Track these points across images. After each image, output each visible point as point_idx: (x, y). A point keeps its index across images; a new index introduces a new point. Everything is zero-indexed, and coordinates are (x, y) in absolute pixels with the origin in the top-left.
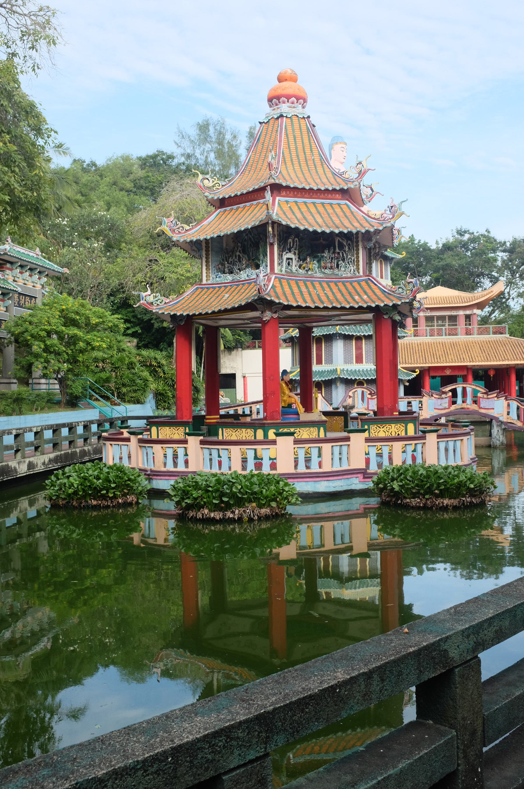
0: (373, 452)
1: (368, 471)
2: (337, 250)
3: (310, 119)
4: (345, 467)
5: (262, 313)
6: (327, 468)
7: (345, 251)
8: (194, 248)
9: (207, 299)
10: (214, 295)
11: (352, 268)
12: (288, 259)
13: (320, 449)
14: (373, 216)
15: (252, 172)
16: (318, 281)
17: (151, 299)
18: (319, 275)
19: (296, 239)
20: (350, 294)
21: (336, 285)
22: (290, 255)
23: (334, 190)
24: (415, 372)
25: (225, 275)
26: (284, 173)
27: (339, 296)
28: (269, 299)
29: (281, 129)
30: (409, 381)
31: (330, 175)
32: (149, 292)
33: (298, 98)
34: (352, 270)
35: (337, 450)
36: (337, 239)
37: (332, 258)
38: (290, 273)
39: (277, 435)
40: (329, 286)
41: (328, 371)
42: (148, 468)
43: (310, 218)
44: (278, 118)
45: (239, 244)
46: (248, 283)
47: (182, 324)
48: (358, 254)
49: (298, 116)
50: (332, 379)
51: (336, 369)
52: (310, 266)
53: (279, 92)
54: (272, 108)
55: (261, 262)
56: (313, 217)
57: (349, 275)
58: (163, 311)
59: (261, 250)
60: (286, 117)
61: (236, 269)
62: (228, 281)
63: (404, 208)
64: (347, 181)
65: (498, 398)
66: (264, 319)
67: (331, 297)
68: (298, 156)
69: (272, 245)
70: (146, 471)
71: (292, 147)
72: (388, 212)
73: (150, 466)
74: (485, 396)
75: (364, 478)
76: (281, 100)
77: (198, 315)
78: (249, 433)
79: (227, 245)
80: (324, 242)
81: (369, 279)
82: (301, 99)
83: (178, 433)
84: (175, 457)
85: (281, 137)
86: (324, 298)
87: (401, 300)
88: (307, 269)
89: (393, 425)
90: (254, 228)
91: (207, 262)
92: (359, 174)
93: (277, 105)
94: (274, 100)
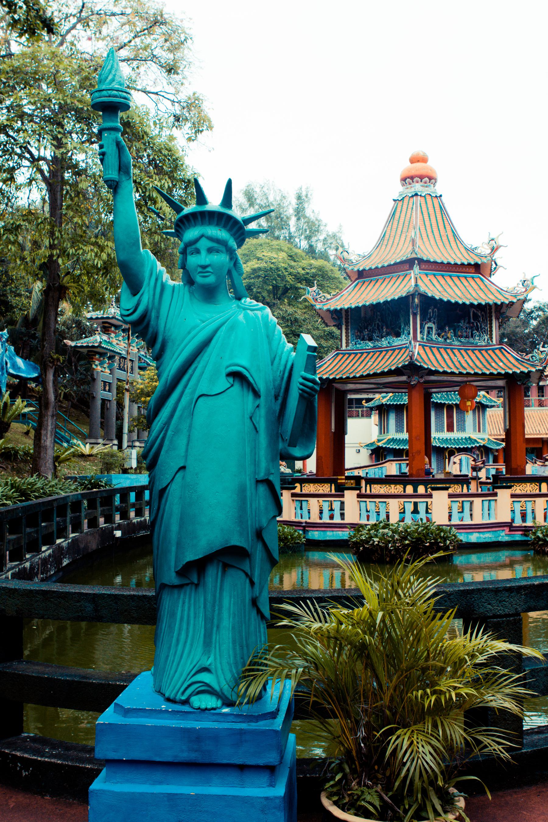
0: (518, 508)
1: (514, 525)
2: (472, 321)
3: (442, 198)
5: (409, 377)
7: (479, 321)
8: (334, 316)
9: (351, 365)
10: (357, 361)
11: (486, 337)
12: (428, 328)
13: (472, 503)
14: (505, 289)
15: (389, 247)
18: (456, 343)
20: (487, 360)
21: (474, 353)
23: (469, 264)
26: (422, 248)
27: (478, 363)
28: (419, 364)
29: (416, 207)
31: (463, 250)
33: (430, 178)
35: (486, 504)
36: (472, 310)
37: (467, 328)
38: (430, 340)
39: (433, 489)
42: (303, 520)
43: (449, 290)
44: (412, 196)
45: (379, 313)
46: (391, 350)
48: (491, 324)
49: (430, 195)
52: (449, 335)
53: (413, 173)
56: (451, 288)
57: (484, 344)
59: (402, 319)
60: (421, 196)
63: (536, 282)
64: (480, 256)
67: (471, 364)
68: (432, 232)
69: (415, 315)
70: (302, 523)
71: (427, 223)
72: (521, 286)
73: (305, 519)
75: (510, 531)
76: (415, 180)
79: (365, 314)
80: (460, 313)
82: (431, 178)
83: (325, 489)
85: (416, 214)
86: (465, 365)
89: (528, 484)
90: (400, 299)
91: (347, 329)
92: (492, 250)
93: (410, 184)
94: (408, 180)
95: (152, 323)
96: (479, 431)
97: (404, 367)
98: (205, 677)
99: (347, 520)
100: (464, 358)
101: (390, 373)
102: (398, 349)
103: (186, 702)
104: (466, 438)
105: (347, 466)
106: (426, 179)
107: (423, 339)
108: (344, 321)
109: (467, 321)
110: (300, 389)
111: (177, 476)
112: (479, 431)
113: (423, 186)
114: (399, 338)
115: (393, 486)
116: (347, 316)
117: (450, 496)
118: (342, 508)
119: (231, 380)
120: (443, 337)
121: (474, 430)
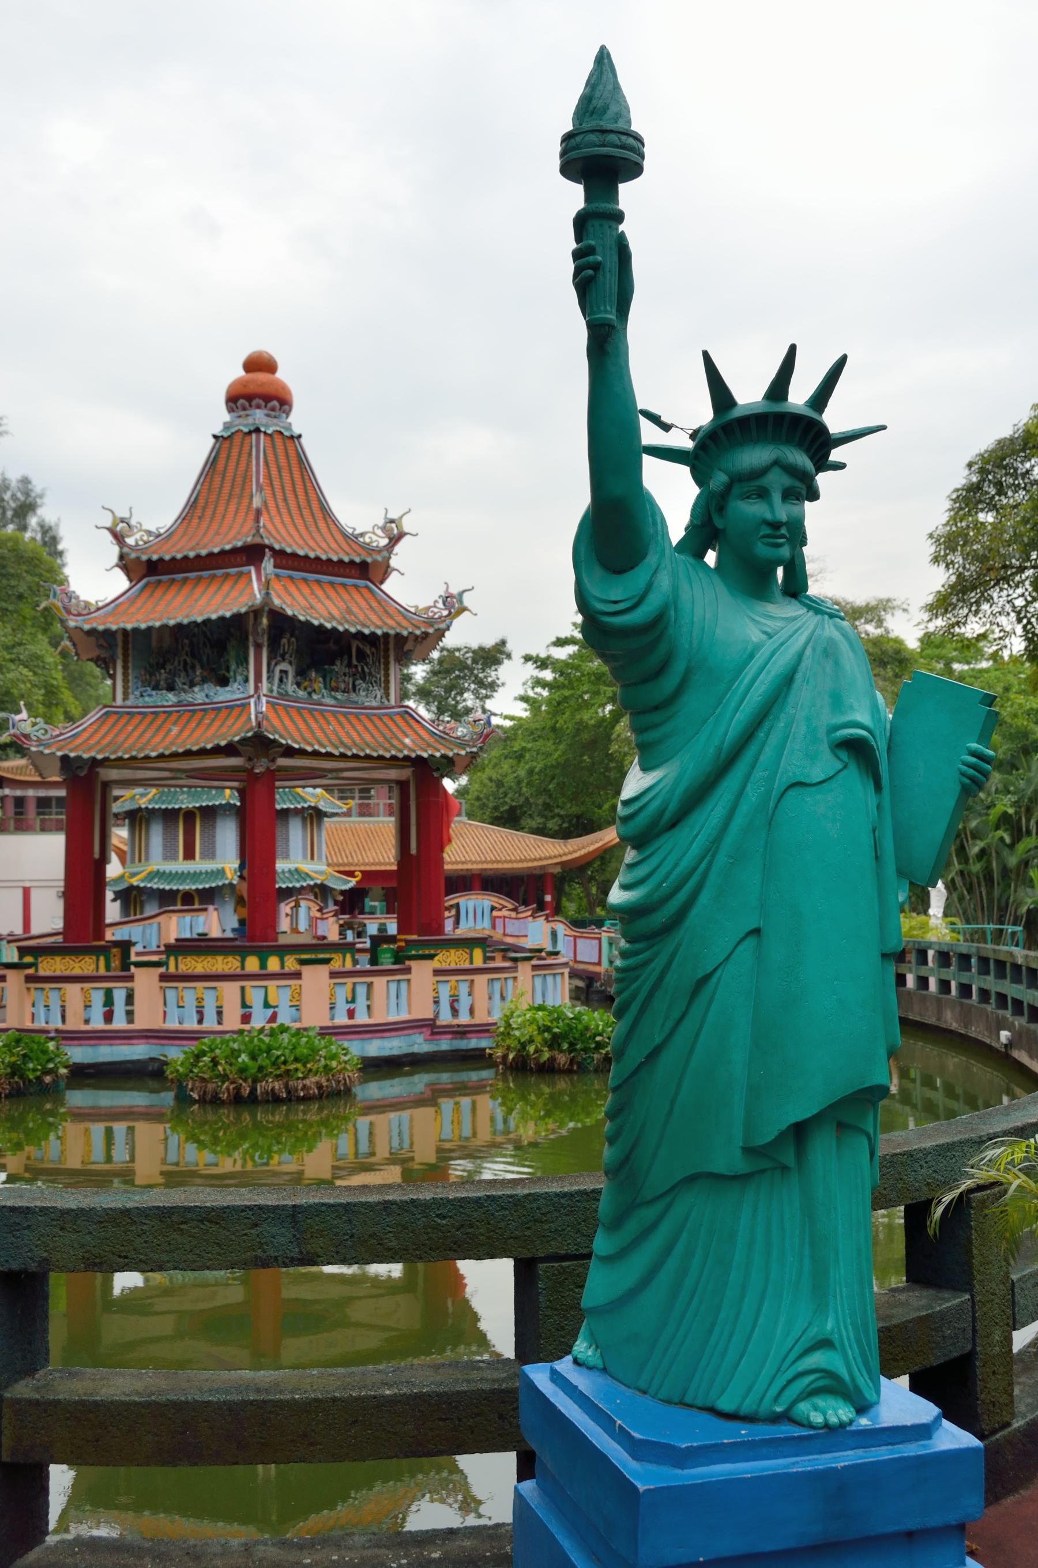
2: (355, 662)
4: (404, 1016)
5: (250, 759)
6: (379, 1018)
12: (281, 671)
13: (370, 986)
14: (413, 610)
16: (329, 711)
17: (26, 728)
18: (328, 701)
19: (293, 639)
22: (284, 666)
23: (352, 562)
24: (354, 877)
25: (159, 692)
26: (269, 526)
28: (271, 737)
30: (343, 893)
31: (338, 537)
32: (24, 715)
34: (379, 696)
35: (393, 987)
36: (355, 644)
38: (284, 696)
39: (303, 962)
40: (347, 719)
41: (207, 873)
44: (250, 433)
45: (186, 641)
47: (82, 774)
49: (281, 433)
50: (217, 887)
51: (223, 869)
52: (316, 686)
53: (252, 389)
54: (235, 414)
55: (232, 674)
57: (374, 704)
58: (53, 750)
59: (232, 653)
60: (265, 433)
61: (179, 682)
62: (170, 703)
63: (468, 600)
64: (368, 549)
65: (534, 918)
66: (257, 771)
68: (285, 500)
69: (258, 647)
70: (47, 1032)
72: (440, 605)
74: (513, 914)
75: (433, 1034)
76: (254, 403)
77: (128, 759)
78: (230, 965)
81: (407, 712)
83: (85, 965)
84: (109, 1001)
86: (346, 740)
87: (464, 749)
88: (309, 690)
92: (391, 539)
93: (244, 409)
94: (242, 401)
95: (671, 631)
96: (312, 858)
97: (244, 741)
98: (817, 1360)
99: (139, 1024)
100: (343, 728)
101: (217, 751)
102: (227, 707)
103: (786, 1417)
104: (290, 871)
105: (108, 921)
106: (275, 403)
107: (271, 691)
108: (120, 651)
109: (346, 662)
110: (963, 774)
111: (741, 948)
112: (312, 858)
113: (268, 416)
114: (228, 688)
115: (220, 958)
116: (125, 643)
117: (333, 975)
118: (130, 999)
119: (844, 755)
120: (305, 689)
121: (305, 856)
